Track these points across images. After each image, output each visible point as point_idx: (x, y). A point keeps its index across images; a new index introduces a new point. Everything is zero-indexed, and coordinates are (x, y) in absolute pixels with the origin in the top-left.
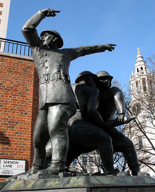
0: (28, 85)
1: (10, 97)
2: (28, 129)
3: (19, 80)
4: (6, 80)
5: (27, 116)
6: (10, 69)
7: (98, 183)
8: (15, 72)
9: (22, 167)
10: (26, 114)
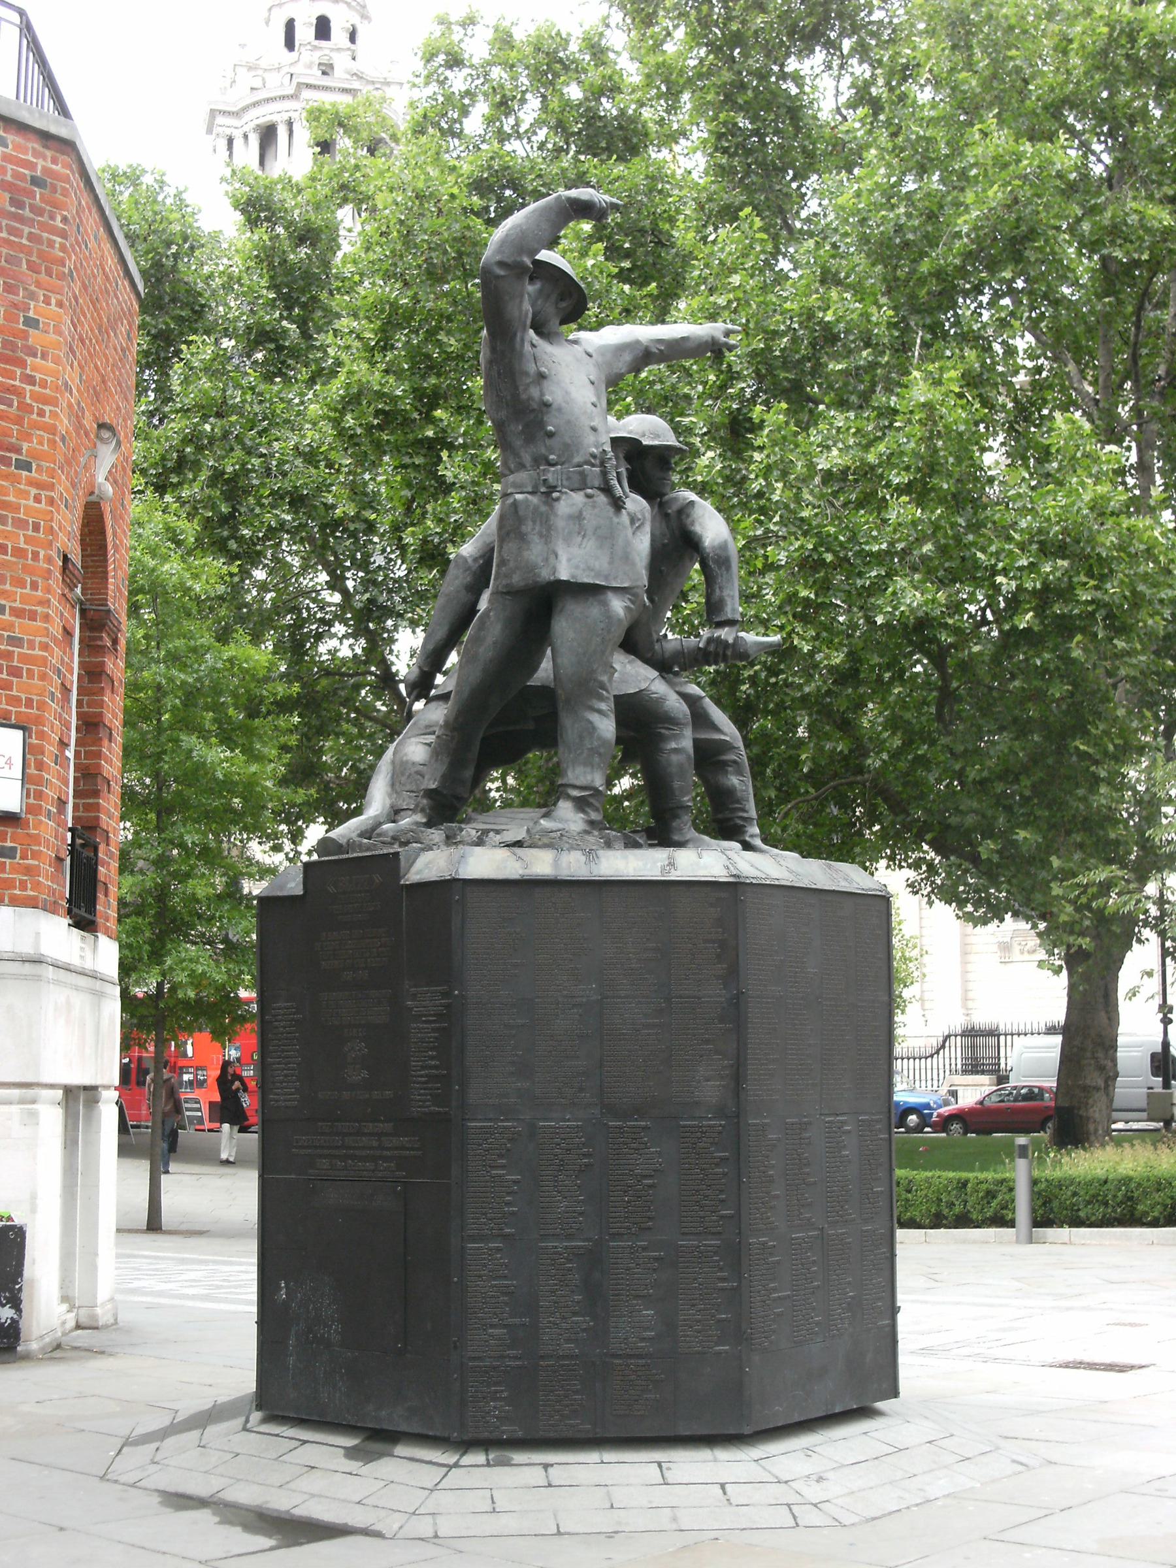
0: (32, 296)
2: (36, 556)
5: (32, 483)
7: (759, 874)
9: (9, 762)
10: (27, 466)
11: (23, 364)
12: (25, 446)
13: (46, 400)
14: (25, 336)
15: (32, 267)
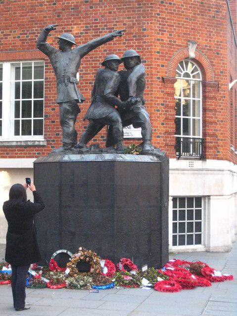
0: (144, 23)
1: (124, 43)
3: (133, 18)
4: (117, 22)
6: (121, 6)
8: (126, 8)
11: (142, 39)
12: (144, 57)
13: (148, 46)
14: (143, 33)
15: (143, 17)
